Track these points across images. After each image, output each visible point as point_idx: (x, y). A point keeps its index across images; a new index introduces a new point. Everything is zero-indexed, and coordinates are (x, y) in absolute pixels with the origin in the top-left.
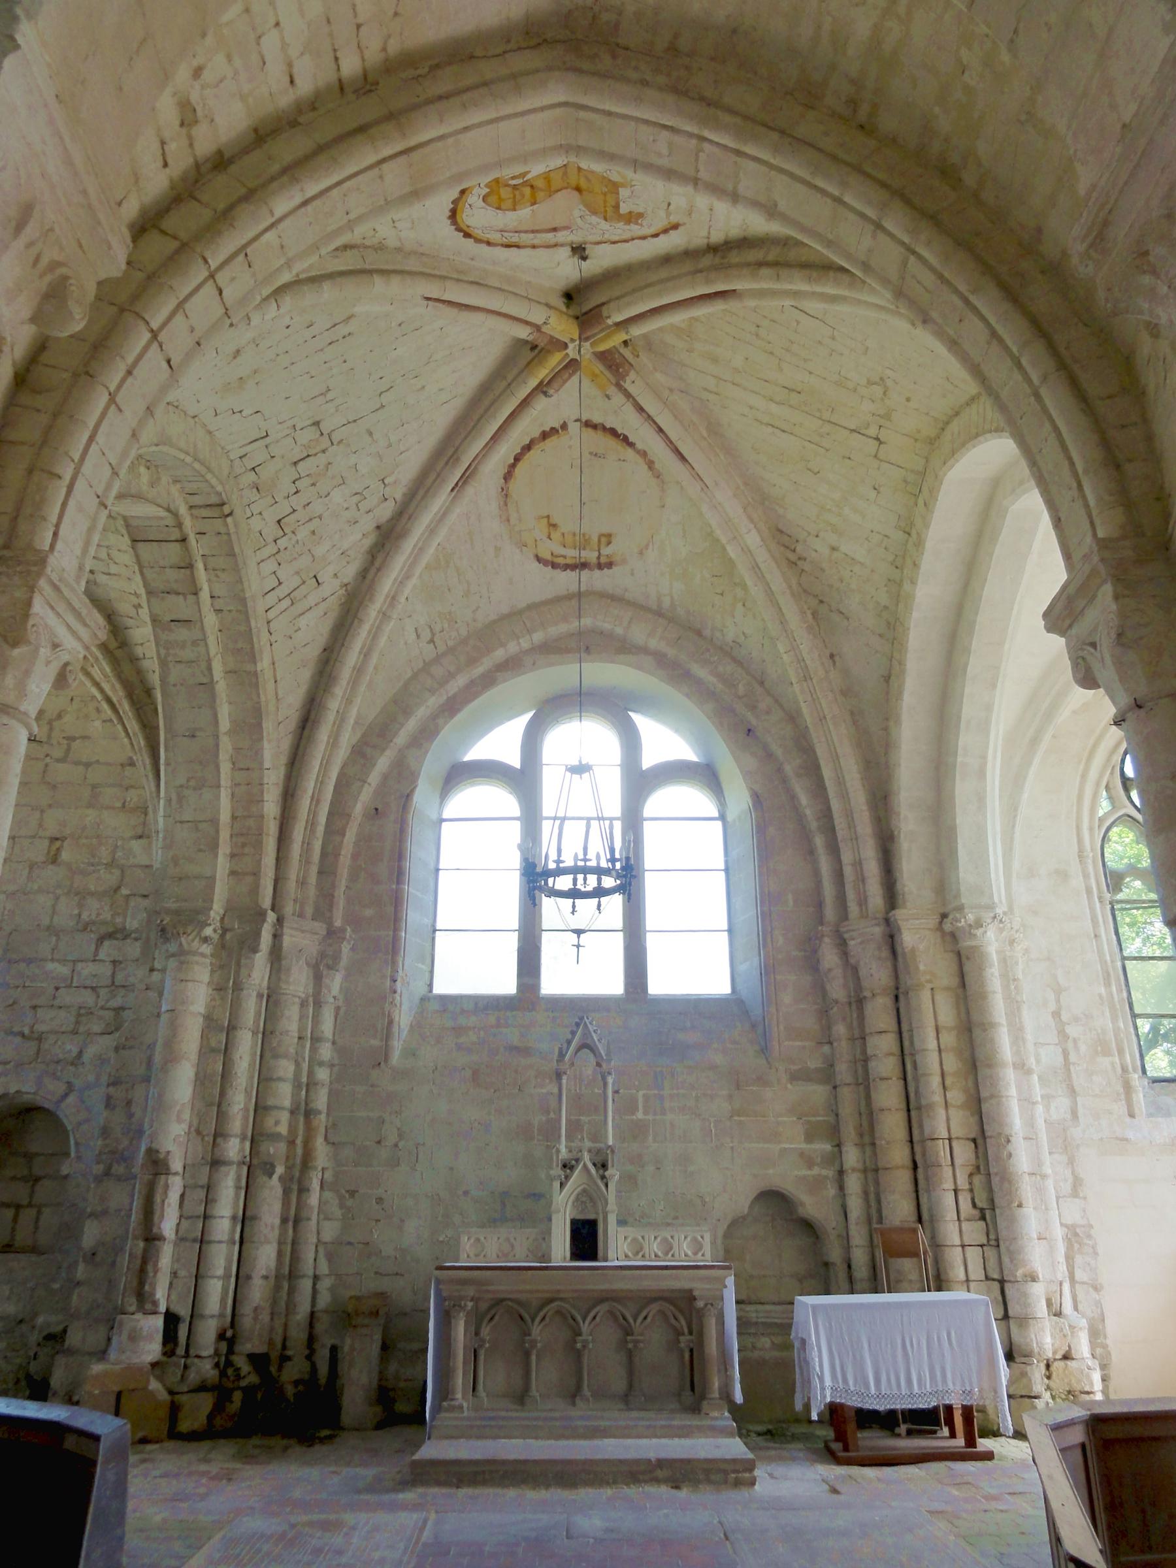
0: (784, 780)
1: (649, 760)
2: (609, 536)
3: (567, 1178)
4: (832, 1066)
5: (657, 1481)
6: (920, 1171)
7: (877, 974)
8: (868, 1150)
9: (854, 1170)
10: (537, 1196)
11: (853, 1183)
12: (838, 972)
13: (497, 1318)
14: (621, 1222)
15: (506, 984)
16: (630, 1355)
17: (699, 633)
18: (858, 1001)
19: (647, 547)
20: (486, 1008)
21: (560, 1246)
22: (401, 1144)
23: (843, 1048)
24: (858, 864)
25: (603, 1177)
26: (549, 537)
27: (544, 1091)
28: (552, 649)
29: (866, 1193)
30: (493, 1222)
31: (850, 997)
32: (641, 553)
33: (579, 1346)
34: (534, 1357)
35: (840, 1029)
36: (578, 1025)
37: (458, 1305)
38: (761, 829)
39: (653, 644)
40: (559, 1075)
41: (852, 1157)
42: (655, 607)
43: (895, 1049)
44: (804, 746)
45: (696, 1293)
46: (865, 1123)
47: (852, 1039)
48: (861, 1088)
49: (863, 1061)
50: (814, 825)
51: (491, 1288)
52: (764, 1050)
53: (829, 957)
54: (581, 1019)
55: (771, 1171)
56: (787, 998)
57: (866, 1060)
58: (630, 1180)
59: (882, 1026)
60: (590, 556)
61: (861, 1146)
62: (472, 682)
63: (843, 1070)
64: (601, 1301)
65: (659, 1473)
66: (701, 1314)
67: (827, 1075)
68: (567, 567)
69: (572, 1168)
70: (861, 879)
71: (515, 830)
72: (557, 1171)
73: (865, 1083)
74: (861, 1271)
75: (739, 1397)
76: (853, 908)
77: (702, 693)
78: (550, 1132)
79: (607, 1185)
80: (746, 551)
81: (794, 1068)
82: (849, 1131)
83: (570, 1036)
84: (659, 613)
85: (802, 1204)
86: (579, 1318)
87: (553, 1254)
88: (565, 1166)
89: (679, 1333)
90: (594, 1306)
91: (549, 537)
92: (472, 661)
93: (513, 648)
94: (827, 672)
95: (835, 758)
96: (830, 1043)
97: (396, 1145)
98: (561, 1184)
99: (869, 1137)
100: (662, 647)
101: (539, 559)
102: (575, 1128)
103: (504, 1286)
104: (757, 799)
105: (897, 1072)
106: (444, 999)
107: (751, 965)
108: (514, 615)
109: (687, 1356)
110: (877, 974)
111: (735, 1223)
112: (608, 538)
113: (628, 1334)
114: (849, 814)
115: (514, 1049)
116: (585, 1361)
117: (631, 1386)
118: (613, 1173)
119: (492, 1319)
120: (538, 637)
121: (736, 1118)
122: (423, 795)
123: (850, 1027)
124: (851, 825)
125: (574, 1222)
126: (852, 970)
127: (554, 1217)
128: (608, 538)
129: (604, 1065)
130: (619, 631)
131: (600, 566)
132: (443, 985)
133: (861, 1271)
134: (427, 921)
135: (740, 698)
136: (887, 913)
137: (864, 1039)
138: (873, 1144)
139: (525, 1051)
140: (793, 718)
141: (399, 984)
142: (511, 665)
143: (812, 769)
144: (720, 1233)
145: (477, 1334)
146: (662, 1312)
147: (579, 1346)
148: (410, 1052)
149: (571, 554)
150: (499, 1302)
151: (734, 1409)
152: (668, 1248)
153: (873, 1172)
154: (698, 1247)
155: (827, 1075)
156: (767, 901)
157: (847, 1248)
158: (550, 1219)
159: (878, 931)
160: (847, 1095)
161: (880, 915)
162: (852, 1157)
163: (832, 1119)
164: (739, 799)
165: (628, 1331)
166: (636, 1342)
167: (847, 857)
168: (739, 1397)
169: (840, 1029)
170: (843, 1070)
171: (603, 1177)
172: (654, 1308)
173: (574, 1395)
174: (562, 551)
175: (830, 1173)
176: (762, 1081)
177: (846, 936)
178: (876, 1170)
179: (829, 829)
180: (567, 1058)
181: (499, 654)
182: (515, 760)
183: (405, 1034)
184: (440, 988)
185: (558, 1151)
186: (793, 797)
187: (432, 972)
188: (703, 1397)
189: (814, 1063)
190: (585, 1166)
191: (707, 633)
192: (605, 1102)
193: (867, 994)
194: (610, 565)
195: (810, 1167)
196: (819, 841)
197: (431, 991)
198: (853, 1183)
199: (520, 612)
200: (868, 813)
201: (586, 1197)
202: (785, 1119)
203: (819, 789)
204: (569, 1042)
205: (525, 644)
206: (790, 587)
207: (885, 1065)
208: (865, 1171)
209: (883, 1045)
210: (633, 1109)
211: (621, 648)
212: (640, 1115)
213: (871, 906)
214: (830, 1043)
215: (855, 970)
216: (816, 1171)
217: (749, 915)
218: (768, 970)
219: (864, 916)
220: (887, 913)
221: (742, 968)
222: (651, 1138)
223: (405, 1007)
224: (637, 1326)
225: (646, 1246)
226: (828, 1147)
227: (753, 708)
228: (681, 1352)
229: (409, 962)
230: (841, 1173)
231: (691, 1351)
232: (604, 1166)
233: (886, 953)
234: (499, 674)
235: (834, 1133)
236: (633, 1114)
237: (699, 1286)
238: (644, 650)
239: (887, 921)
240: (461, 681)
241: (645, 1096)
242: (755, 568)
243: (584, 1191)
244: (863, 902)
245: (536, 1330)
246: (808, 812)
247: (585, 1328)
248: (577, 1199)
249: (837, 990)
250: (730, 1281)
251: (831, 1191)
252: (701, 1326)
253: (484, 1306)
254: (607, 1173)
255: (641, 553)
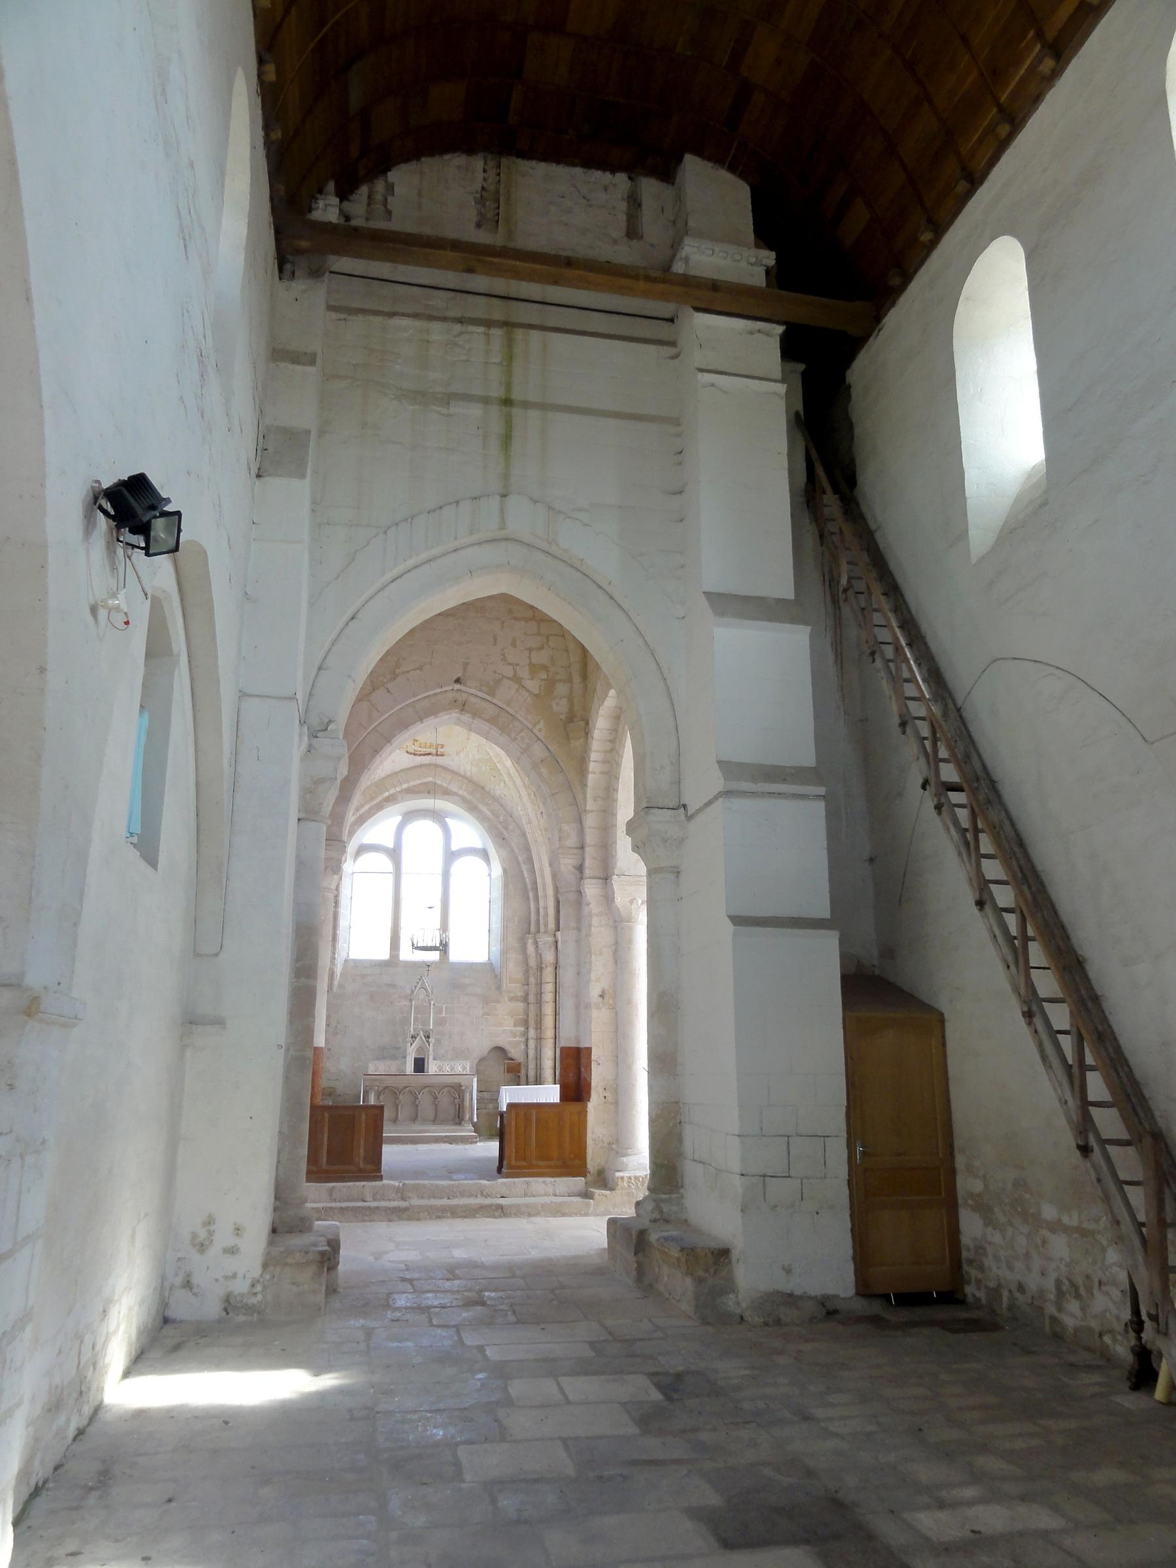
0: (518, 863)
1: (455, 847)
2: (443, 745)
3: (413, 1041)
4: (528, 995)
5: (445, 1142)
6: (557, 1040)
7: (549, 957)
8: (539, 1030)
9: (532, 1038)
10: (398, 1049)
11: (532, 1044)
12: (534, 954)
13: (386, 1094)
14: (434, 1059)
15: (384, 954)
16: (436, 1105)
17: (483, 788)
18: (540, 968)
19: (461, 752)
20: (375, 965)
21: (410, 1068)
22: (338, 1026)
23: (533, 989)
24: (546, 908)
25: (428, 1042)
26: (414, 744)
27: (402, 1004)
28: (412, 792)
29: (536, 1048)
30: (377, 1059)
31: (537, 965)
32: (457, 754)
33: (417, 1103)
34: (400, 1107)
35: (532, 980)
36: (420, 979)
37: (371, 1088)
38: (506, 886)
39: (461, 792)
40: (411, 1000)
41: (532, 1033)
42: (463, 774)
43: (553, 990)
44: (527, 849)
45: (462, 1084)
46: (539, 1019)
47: (536, 984)
48: (538, 1005)
49: (540, 994)
50: (529, 887)
51: (385, 1082)
52: (499, 988)
53: (531, 949)
54: (421, 977)
55: (498, 1039)
56: (511, 965)
57: (541, 993)
58: (438, 1042)
59: (549, 980)
60: (434, 751)
61: (536, 1029)
62: (370, 809)
63: (532, 998)
64: (425, 1087)
65: (446, 1140)
66: (463, 1092)
67: (525, 999)
68: (421, 755)
69: (415, 1038)
70: (546, 915)
71: (390, 879)
72: (409, 1039)
73: (539, 1003)
74: (531, 1079)
75: (475, 1119)
76: (542, 929)
77: (482, 818)
78: (405, 1021)
79: (429, 1045)
80: (505, 766)
81: (512, 995)
82: (532, 1023)
83: (416, 984)
84: (464, 777)
85: (510, 1052)
86: (418, 1094)
87: (407, 1071)
88: (412, 1037)
89: (455, 1098)
90: (422, 1089)
91: (414, 744)
92: (372, 799)
93: (392, 791)
94: (538, 821)
95: (540, 860)
96: (528, 985)
97: (336, 1027)
98: (411, 1044)
99: (539, 1026)
100: (465, 794)
101: (407, 752)
102: (416, 1019)
103: (390, 1082)
104: (505, 871)
105: (553, 999)
106: (355, 961)
107: (496, 948)
108: (395, 774)
109: (457, 1106)
110: (549, 957)
111: (482, 1060)
112: (442, 746)
113: (435, 1099)
114: (544, 885)
115: (389, 985)
116: (419, 1108)
117: (436, 1116)
118: (432, 1040)
119: (384, 1094)
120: (405, 786)
121: (485, 1017)
122: (348, 866)
123: (537, 979)
124: (544, 890)
125: (415, 1059)
126: (539, 956)
127: (408, 1057)
128: (442, 746)
129: (430, 996)
130: (445, 785)
131: (437, 755)
132: (354, 955)
133: (531, 1079)
134: (347, 924)
135: (500, 823)
136: (556, 931)
137: (541, 984)
138: (541, 1028)
139: (392, 985)
140: (524, 835)
141: (336, 955)
142: (391, 800)
143: (530, 860)
144: (475, 1063)
145: (378, 1099)
146: (449, 1091)
147: (417, 1103)
148: (341, 986)
149: (423, 750)
150: (387, 1087)
151: (474, 1125)
152: (452, 1069)
153: (539, 1039)
154: (465, 1068)
155: (525, 999)
156: (506, 920)
157: (527, 1070)
158: (405, 1057)
159: (551, 939)
160: (532, 1007)
161: (553, 933)
162: (532, 1033)
163: (526, 1017)
164: (497, 870)
165: (436, 1098)
166: (438, 1101)
167: (541, 904)
168: (475, 1119)
169: (532, 980)
170: (532, 998)
171: (428, 1042)
172: (446, 1090)
173: (414, 1119)
174: (420, 749)
175: (523, 1039)
176: (498, 1001)
177: (538, 940)
178: (541, 1039)
179: (535, 889)
180: (415, 994)
181: (386, 794)
182: (390, 844)
183: (338, 978)
184: (351, 957)
185: (410, 1031)
186: (522, 872)
187: (349, 947)
188: (462, 1120)
189: (519, 994)
190: (421, 1037)
191: (487, 789)
192: (430, 1008)
193: (543, 966)
194: (442, 755)
195: (515, 1038)
196: (531, 895)
197: (348, 956)
198: (532, 1044)
199: (397, 773)
200: (552, 886)
201: (420, 1049)
202: (506, 1017)
203: (532, 871)
204: (416, 987)
205: (398, 789)
206: (524, 784)
207: (548, 997)
208: (536, 1039)
209: (549, 988)
210: (441, 1013)
211: (446, 793)
212: (444, 1015)
213: (549, 927)
214: (528, 985)
215: (541, 955)
216: (517, 1039)
217: (497, 925)
218: (504, 953)
219: (546, 932)
220: (556, 931)
221: (493, 949)
222: (448, 1025)
223: (339, 966)
224: (439, 1096)
225: (444, 1068)
226: (523, 1029)
227: (506, 828)
228: (456, 1105)
229: (341, 944)
230: (527, 1039)
231: (459, 1105)
232: (428, 1037)
233: (553, 949)
234: (385, 803)
235: (526, 1023)
236: (440, 1014)
237: (463, 1081)
238: (456, 794)
239: (555, 935)
240: (367, 807)
241: (446, 1007)
242: (509, 774)
243: (420, 1047)
244: (546, 925)
245: (401, 1097)
246: (527, 880)
247: (420, 1097)
248: (417, 1049)
249: (533, 962)
250: (475, 1080)
251: (523, 1047)
252: (463, 1097)
253: (380, 1089)
254: (430, 1040)
255: (457, 754)
